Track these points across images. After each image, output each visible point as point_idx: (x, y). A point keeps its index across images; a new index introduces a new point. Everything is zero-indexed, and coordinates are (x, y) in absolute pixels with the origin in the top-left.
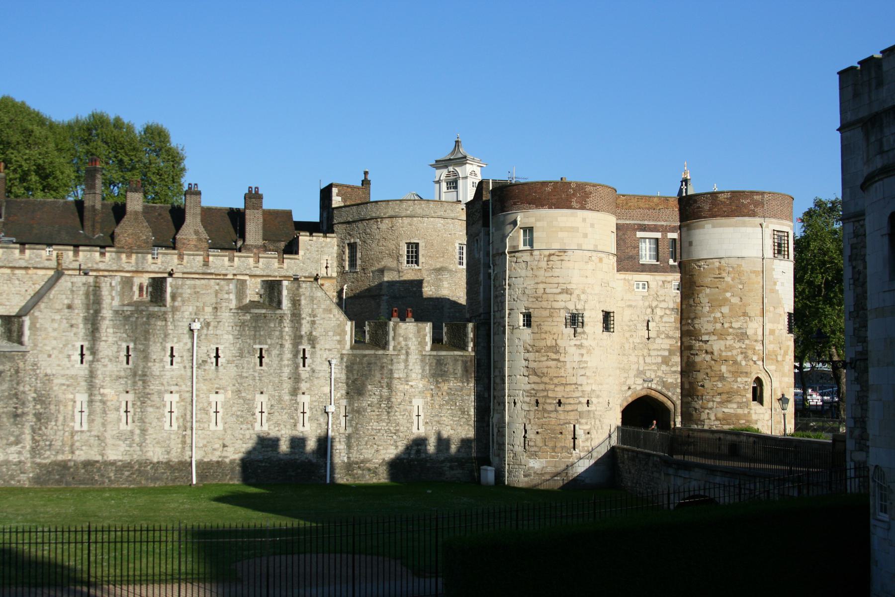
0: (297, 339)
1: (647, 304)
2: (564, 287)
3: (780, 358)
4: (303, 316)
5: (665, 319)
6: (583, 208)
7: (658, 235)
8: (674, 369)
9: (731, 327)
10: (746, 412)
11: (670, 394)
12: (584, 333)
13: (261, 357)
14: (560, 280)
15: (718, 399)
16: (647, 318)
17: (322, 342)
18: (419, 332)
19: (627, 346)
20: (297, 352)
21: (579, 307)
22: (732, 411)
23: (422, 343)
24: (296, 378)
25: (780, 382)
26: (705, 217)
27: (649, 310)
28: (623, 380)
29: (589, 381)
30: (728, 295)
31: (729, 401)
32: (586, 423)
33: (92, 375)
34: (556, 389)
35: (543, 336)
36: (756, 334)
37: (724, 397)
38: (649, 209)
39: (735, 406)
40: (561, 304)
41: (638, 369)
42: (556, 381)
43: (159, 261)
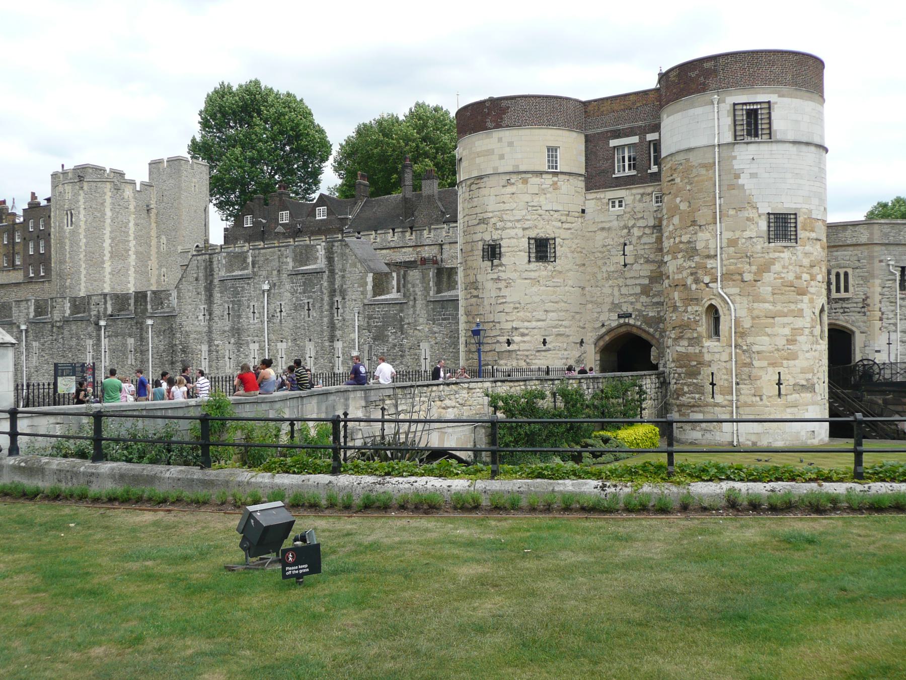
0: (332, 293)
1: (622, 224)
2: (481, 216)
3: (747, 277)
4: (337, 271)
5: (644, 240)
6: (498, 126)
7: (635, 139)
8: (655, 300)
9: (681, 242)
10: (697, 351)
11: (651, 330)
13: (309, 310)
14: (478, 210)
16: (622, 241)
17: (350, 293)
18: (423, 278)
19: (599, 276)
20: (333, 303)
21: (495, 237)
22: (682, 350)
23: (427, 289)
24: (332, 326)
25: (751, 310)
27: (626, 231)
28: (596, 315)
30: (678, 200)
31: (681, 338)
32: (506, 365)
33: (210, 332)
35: (469, 272)
36: (706, 247)
37: (678, 330)
38: (624, 110)
39: (686, 343)
40: (478, 237)
41: (613, 303)
43: (432, 235)
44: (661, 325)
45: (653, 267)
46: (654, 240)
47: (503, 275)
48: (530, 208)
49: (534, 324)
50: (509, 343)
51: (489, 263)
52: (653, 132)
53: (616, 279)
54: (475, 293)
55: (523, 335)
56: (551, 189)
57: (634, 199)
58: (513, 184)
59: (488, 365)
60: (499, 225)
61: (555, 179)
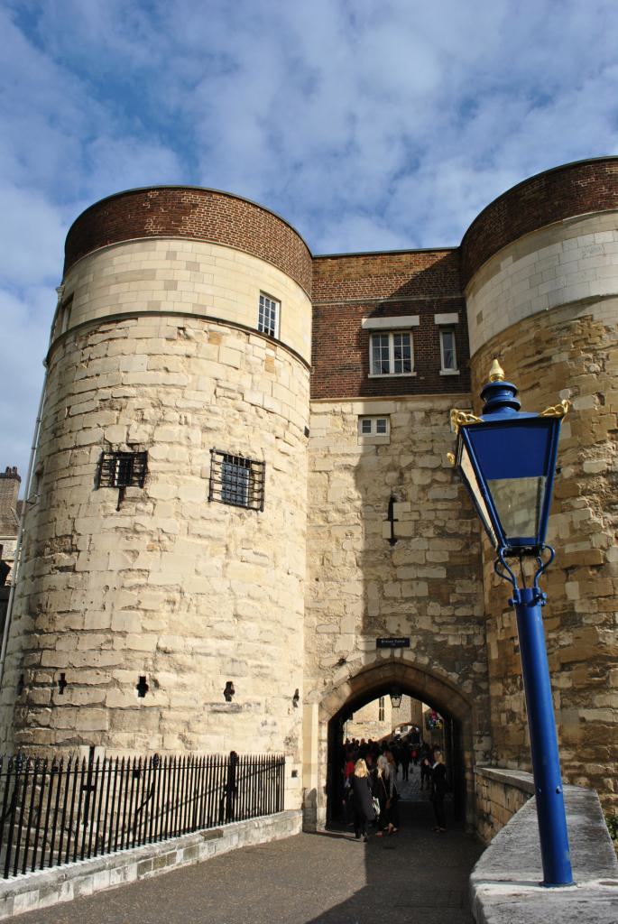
1: (387, 461)
2: (106, 393)
5: (432, 494)
6: (171, 231)
7: (413, 320)
9: (582, 475)
11: (454, 677)
12: (146, 499)
15: (564, 682)
16: (387, 492)
19: (337, 559)
21: (135, 437)
26: (500, 247)
27: (394, 475)
28: (327, 639)
29: (149, 625)
32: (131, 745)
34: (59, 646)
40: (95, 435)
42: (61, 624)
44: (477, 667)
45: (455, 545)
46: (455, 494)
47: (146, 522)
48: (220, 392)
49: (212, 644)
50: (142, 688)
51: (114, 494)
52: (446, 309)
53: (374, 566)
54: (65, 559)
55: (180, 669)
56: (262, 369)
57: (412, 419)
58: (188, 338)
59: (80, 742)
60: (150, 413)
61: (272, 353)
